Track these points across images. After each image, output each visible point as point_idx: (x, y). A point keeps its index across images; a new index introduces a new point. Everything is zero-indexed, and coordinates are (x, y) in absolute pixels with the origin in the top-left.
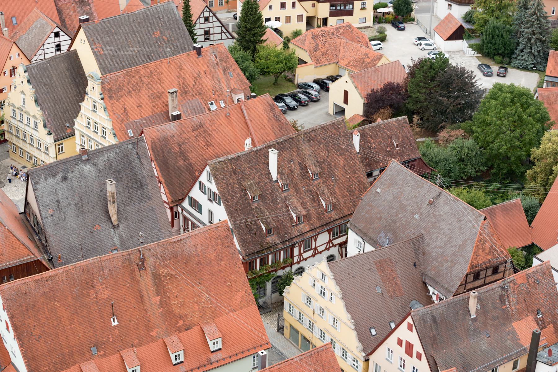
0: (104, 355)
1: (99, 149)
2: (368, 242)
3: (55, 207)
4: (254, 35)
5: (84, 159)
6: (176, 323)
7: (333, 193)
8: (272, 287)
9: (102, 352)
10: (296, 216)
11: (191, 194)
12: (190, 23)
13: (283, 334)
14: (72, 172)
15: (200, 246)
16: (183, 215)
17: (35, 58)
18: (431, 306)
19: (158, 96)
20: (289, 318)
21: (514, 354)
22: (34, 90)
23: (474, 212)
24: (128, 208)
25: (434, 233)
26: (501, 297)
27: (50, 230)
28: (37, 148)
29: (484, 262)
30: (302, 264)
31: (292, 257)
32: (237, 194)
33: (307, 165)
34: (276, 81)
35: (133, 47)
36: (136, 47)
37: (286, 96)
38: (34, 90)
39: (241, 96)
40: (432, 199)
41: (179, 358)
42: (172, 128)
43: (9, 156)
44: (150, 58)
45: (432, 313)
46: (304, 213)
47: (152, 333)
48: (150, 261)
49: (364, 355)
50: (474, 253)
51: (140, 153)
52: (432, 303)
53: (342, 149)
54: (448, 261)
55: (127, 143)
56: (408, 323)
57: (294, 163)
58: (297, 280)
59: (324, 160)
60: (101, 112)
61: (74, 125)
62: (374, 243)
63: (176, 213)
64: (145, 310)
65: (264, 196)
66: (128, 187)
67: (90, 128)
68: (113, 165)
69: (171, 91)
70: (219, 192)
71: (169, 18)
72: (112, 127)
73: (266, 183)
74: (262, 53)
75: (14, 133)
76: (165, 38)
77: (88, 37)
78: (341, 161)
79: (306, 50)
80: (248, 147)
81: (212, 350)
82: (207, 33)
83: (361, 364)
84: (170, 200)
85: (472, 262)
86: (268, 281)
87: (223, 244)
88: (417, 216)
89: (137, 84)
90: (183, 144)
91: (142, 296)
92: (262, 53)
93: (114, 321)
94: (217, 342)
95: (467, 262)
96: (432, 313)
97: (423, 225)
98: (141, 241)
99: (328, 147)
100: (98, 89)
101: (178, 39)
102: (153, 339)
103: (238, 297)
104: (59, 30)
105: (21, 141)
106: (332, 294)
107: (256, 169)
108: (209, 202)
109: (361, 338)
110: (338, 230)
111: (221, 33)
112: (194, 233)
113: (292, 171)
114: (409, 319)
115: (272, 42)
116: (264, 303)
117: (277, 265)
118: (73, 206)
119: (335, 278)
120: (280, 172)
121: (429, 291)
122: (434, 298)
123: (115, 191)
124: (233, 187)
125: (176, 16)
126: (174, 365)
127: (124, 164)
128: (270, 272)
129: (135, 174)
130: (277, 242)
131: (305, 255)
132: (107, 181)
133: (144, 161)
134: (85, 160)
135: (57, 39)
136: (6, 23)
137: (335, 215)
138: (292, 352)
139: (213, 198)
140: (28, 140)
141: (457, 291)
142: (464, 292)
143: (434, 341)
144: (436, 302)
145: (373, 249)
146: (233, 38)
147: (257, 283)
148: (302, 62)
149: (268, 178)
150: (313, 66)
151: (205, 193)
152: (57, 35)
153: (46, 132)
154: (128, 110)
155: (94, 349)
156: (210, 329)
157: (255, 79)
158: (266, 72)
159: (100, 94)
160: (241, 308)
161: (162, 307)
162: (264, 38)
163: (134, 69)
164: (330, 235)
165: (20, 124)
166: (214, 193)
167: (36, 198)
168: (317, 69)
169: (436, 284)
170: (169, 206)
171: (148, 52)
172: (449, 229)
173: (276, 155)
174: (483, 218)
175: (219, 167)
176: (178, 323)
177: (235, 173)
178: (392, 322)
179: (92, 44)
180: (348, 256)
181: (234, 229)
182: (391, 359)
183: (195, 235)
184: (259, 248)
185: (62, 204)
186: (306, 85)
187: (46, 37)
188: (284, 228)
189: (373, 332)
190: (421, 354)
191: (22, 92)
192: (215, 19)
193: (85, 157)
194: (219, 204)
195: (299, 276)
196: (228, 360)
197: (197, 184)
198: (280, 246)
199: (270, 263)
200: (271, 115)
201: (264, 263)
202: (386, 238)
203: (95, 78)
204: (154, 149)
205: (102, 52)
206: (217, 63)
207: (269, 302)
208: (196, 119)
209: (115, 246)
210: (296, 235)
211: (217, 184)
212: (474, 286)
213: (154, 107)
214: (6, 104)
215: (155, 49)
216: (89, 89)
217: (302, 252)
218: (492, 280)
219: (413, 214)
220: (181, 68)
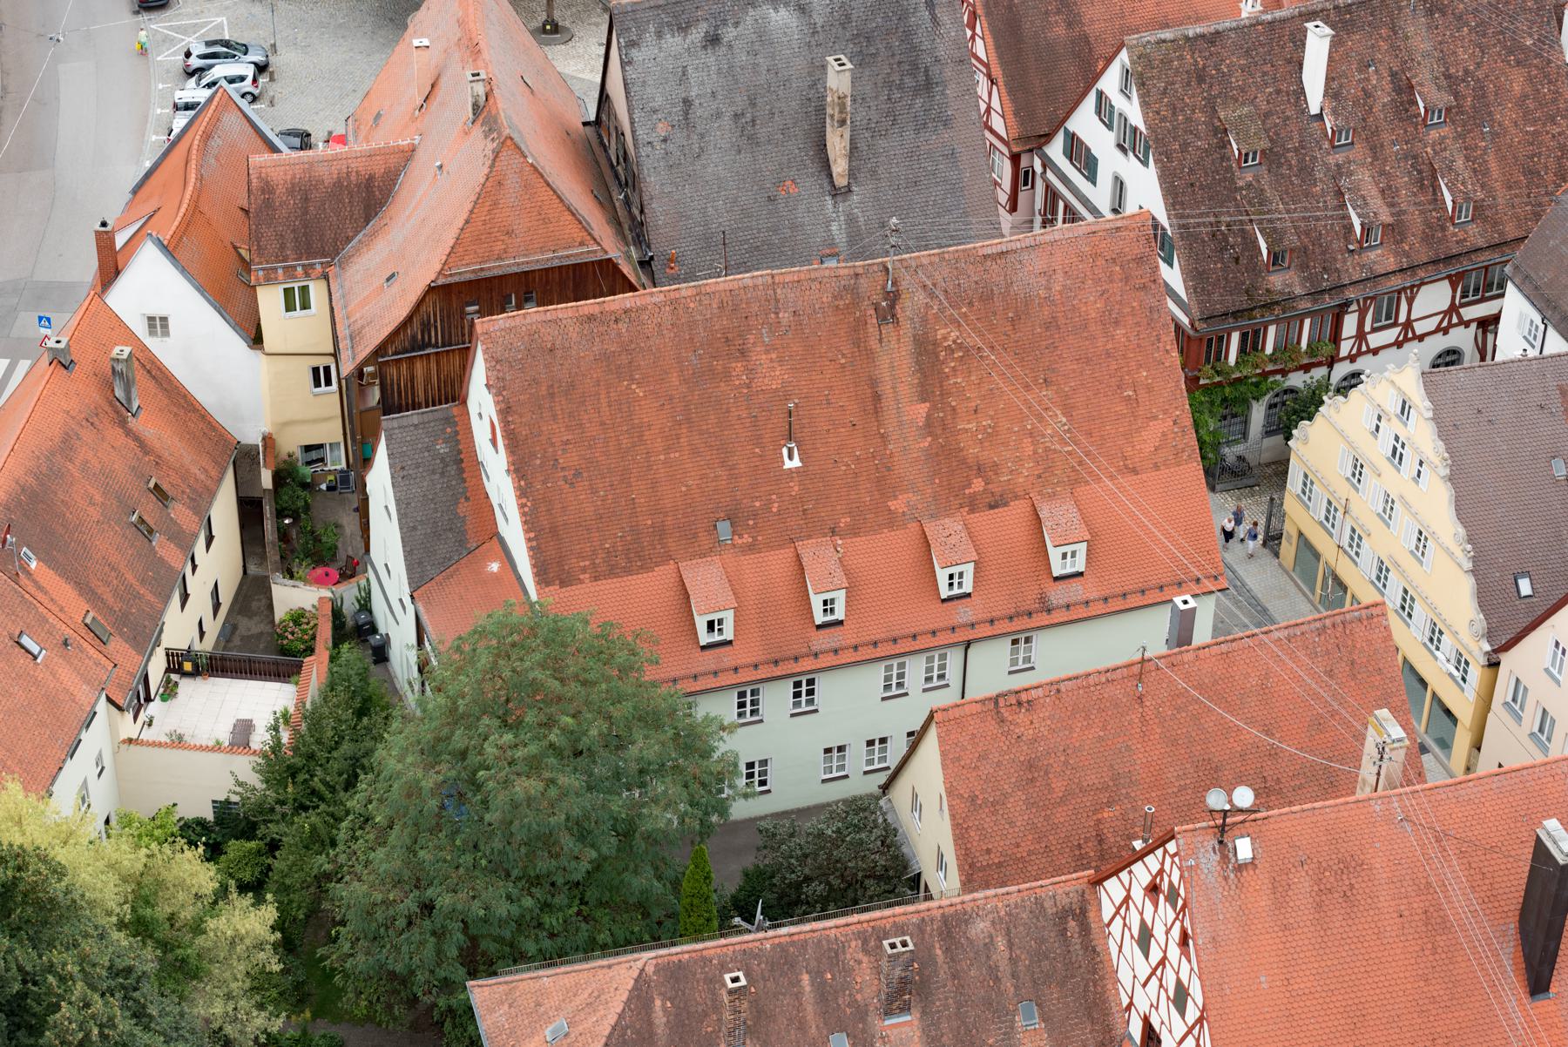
0: (751, 548)
2: (1555, 327)
3: (677, 118)
6: (965, 483)
7: (1480, 172)
8: (1268, 416)
9: (747, 539)
11: (1073, 125)
13: (1277, 555)
14: (736, 24)
15: (1060, 276)
16: (1045, 180)
20: (1299, 515)
24: (882, 143)
27: (654, 180)
30: (1361, 363)
31: (1336, 339)
32: (1199, 139)
33: (1414, 82)
46: (1385, 217)
47: (892, 505)
48: (913, 302)
49: (1487, 648)
53: (1524, 49)
57: (1376, 71)
58: (1332, 407)
59: (1466, 72)
63: (1027, 173)
64: (882, 436)
66: (889, 84)
70: (1149, 127)
73: (1288, 118)
78: (1517, 83)
81: (1055, 574)
83: (1476, 673)
84: (1014, 134)
86: (1244, 396)
87: (1127, 279)
91: (877, 397)
93: (791, 457)
94: (1074, 554)
98: (893, 241)
99: (1484, 35)
102: (892, 521)
106: (1421, 463)
107: (1265, 74)
108: (1118, 154)
109: (1485, 599)
110: (1478, 281)
112: (1048, 238)
113: (1367, 94)
116: (1241, 458)
118: (727, 120)
119: (1436, 419)
120: (1332, 91)
123: (848, 91)
124: (1188, 120)
126: (944, 601)
127: (886, 18)
128: (1265, 375)
129: (914, 48)
130: (1298, 291)
131: (1375, 340)
132: (830, 59)
137: (1475, 235)
138: (1292, 606)
139: (1129, 143)
147: (1225, 400)
151: (1109, 127)
155: (724, 528)
156: (1058, 514)
160: (1156, 467)
161: (930, 434)
164: (1454, 291)
166: (1135, 129)
167: (625, 85)
173: (1326, 43)
175: (1157, 56)
176: (969, 485)
177: (1201, 79)
180: (1498, 358)
182: (1560, 672)
183: (1052, 243)
184: (1241, 301)
185: (698, 112)
188: (1324, 253)
189: (1525, 587)
194: (1145, 163)
195: (1340, 398)
196: (1099, 608)
197: (1091, 99)
198: (1305, 305)
199: (1269, 349)
201: (1251, 343)
209: (833, 245)
211: (1145, 105)
217: (1367, 328)
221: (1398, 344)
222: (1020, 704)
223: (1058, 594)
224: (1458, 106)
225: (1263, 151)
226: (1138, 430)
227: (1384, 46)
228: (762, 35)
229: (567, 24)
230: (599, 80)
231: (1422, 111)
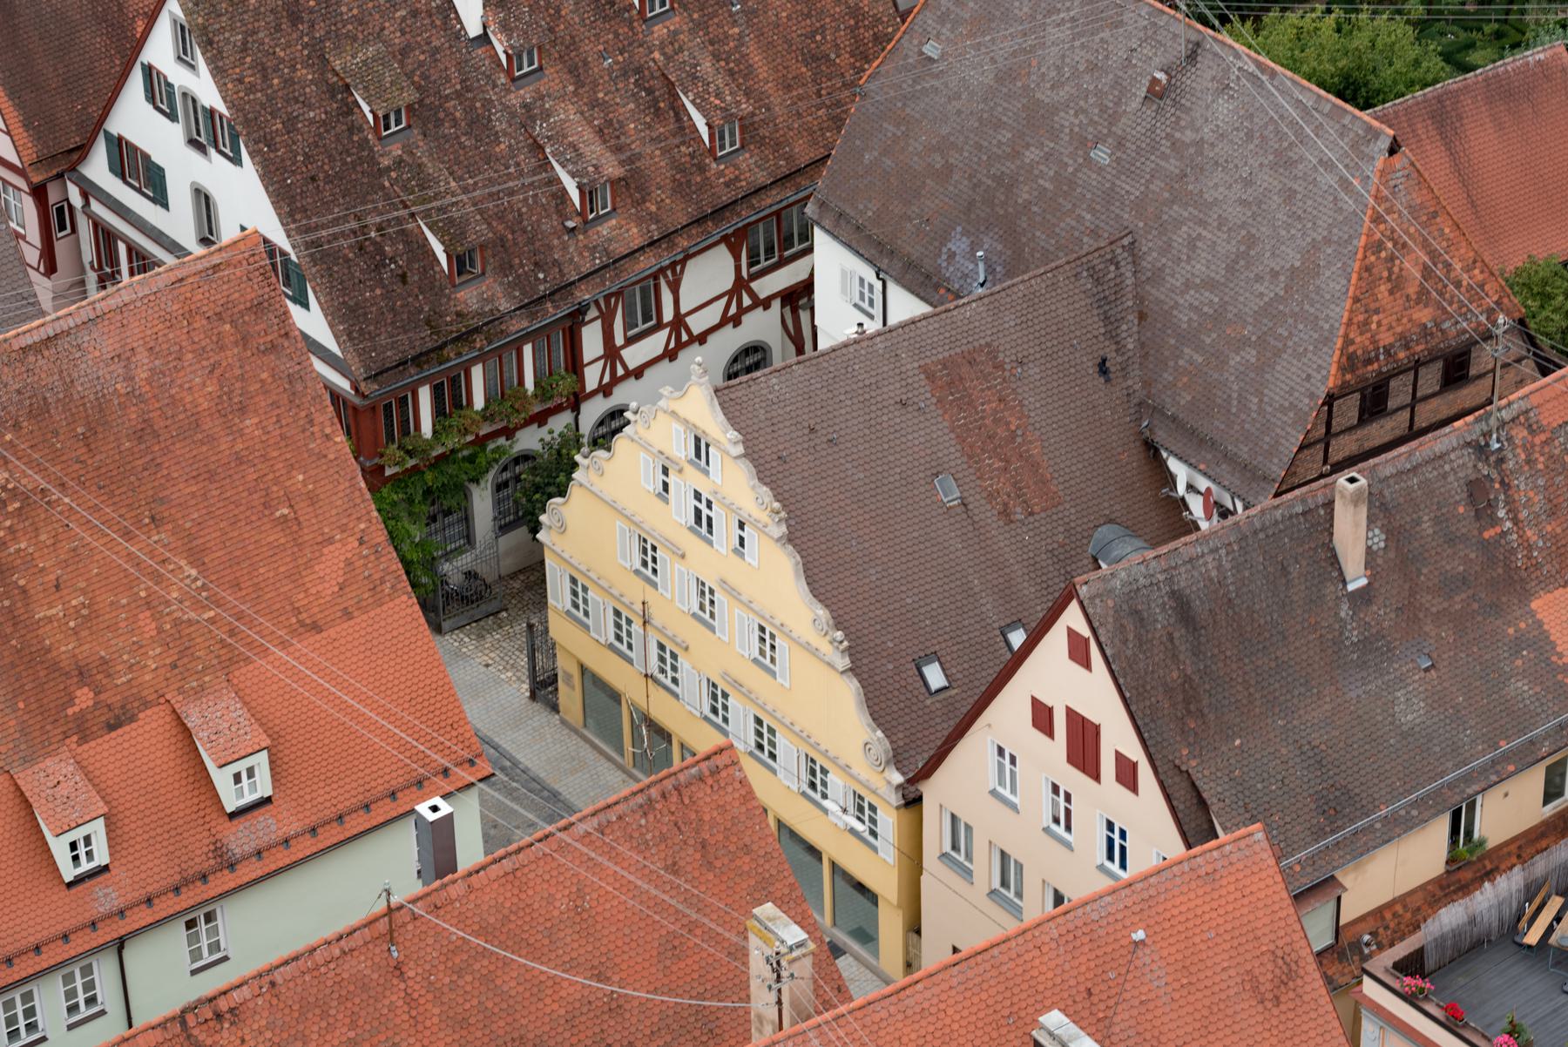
2: (900, 281)
7: (739, 73)
8: (498, 503)
10: (580, 187)
13: (555, 708)
15: (142, 356)
18: (1188, 539)
20: (576, 642)
21: (1547, 736)
23: (1347, 120)
25: (1178, 223)
26: (1476, 489)
29: (1402, 336)
30: (620, 395)
31: (575, 365)
32: (311, 107)
40: (1160, 76)
41: (89, 854)
45: (1170, 581)
46: (612, 168)
49: (898, 778)
50: (1356, 300)
52: (1189, 532)
54: (1244, 342)
56: (1070, 630)
58: (591, 471)
62: (923, 282)
63: (60, 211)
73: (437, 50)
81: (230, 809)
83: (889, 821)
84: (31, 154)
85: (1348, 341)
87: (244, 341)
88: (1101, 155)
94: (251, 772)
95: (1327, 341)
96: (1170, 581)
97: (1131, 188)
103: (330, 566)
106: (741, 526)
108: (193, 155)
109: (879, 707)
110: (769, 235)
112: (112, 302)
114: (1073, 617)
116: (470, 575)
117: (511, 409)
119: (752, 454)
121: (1171, 480)
122: (1196, 505)
124: (288, 82)
126: (70, 885)
128: (481, 441)
130: (504, 305)
131: (634, 356)
137: (752, 168)
138: (595, 780)
139: (206, 134)
141: (1290, 472)
142: (1322, 476)
143: (1187, 702)
144: (1204, 525)
145: (924, 308)
147: (428, 492)
149: (446, 25)
151: (172, 116)
156: (215, 717)
160: (347, 615)
164: (737, 258)
166: (211, 113)
169: (1200, 448)
170: (29, 183)
172: (1243, 203)
174: (1384, 144)
176: (71, 701)
177: (295, 19)
178: (1013, 626)
180: (823, 344)
181: (305, 262)
182: (1013, 791)
183: (121, 309)
184: (423, 339)
188: (531, 241)
189: (935, 676)
190: (1135, 765)
194: (236, 160)
195: (601, 453)
196: (307, 846)
197: (136, 82)
198: (519, 325)
199: (479, 402)
201: (450, 399)
202: (974, 260)
207: (487, 572)
210: (586, 269)
211: (218, 73)
212: (1368, 445)
217: (619, 340)
218: (1445, 413)
219: (1084, 144)
221: (670, 355)
222: (219, 1016)
223: (240, 838)
225: (409, 108)
226: (308, 565)
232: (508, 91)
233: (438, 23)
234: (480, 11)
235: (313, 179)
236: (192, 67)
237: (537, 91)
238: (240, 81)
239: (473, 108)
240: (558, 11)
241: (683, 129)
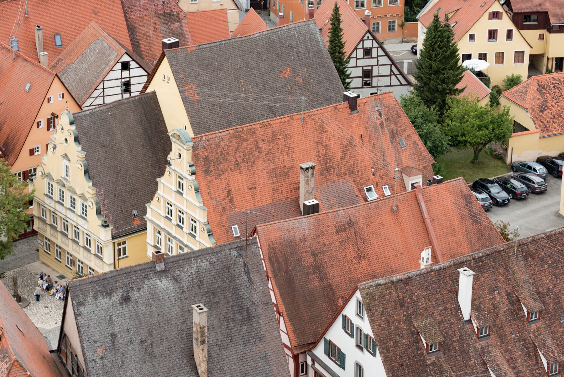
1: (184, 255)
3: (108, 345)
4: (443, 81)
5: (158, 269)
11: (329, 336)
12: (340, 58)
14: (139, 289)
16: (314, 369)
17: (88, 103)
19: (284, 174)
22: (85, 153)
24: (225, 353)
28: (84, 248)
32: (404, 339)
33: (520, 297)
34: (476, 157)
35: (246, 92)
36: (252, 92)
37: (492, 182)
38: (85, 153)
39: (419, 180)
42: (303, 225)
43: (38, 258)
44: (273, 112)
51: (249, 264)
55: (229, 247)
57: (499, 293)
59: (548, 289)
60: (189, 194)
61: (145, 213)
63: (303, 365)
65: (447, 344)
66: (227, 319)
67: (170, 220)
68: (205, 282)
69: (304, 166)
70: (375, 334)
71: (307, 47)
72: (206, 220)
73: (452, 323)
74: (455, 111)
75: (48, 222)
76: (300, 79)
77: (175, 72)
79: (526, 110)
80: (425, 263)
82: (367, 74)
84: (295, 343)
89: (250, 153)
90: (320, 252)
92: (456, 110)
99: (556, 269)
100: (187, 156)
101: (320, 83)
104: (131, 60)
105: (59, 235)
108: (358, 351)
111: (390, 75)
113: (495, 307)
115: (472, 94)
118: (136, 344)
120: (475, 307)
124: (397, 328)
125: (318, 45)
129: (240, 297)
132: (194, 306)
133: (256, 278)
134: (161, 271)
135: (126, 74)
136: (45, 44)
139: (364, 343)
140: (71, 234)
146: (409, 83)
148: (519, 128)
150: (538, 135)
151: (351, 336)
152: (125, 66)
153: (100, 223)
154: (234, 194)
157: (442, 153)
158: (460, 142)
159: (191, 166)
162: (459, 86)
163: (246, 127)
165: (59, 207)
166: (367, 336)
167: (78, 327)
168: (544, 141)
170: (292, 353)
171: (270, 101)
173: (471, 278)
175: (377, 293)
177: (402, 305)
179: (181, 84)
186: (524, 165)
187: (107, 69)
191: (66, 156)
192: (381, 53)
193: (160, 267)
194: (374, 355)
197: (339, 321)
200: (466, 212)
203: (183, 139)
204: (272, 259)
205: (197, 97)
206: (382, 124)
208: (343, 214)
211: (372, 321)
213: (276, 190)
214: (39, 173)
215: (282, 97)
216: (172, 156)
220: (322, 129)
224: (546, 309)
225: (440, 344)
227: (502, 279)
228: (153, 294)
229: (25, 296)
230: (60, 324)
231: (526, 313)
232: (476, 342)
233: (454, 313)
234: (470, 311)
235: (402, 365)
236: (362, 318)
237: (487, 343)
238: (380, 325)
239: (463, 346)
240: (498, 315)
241: (538, 363)
